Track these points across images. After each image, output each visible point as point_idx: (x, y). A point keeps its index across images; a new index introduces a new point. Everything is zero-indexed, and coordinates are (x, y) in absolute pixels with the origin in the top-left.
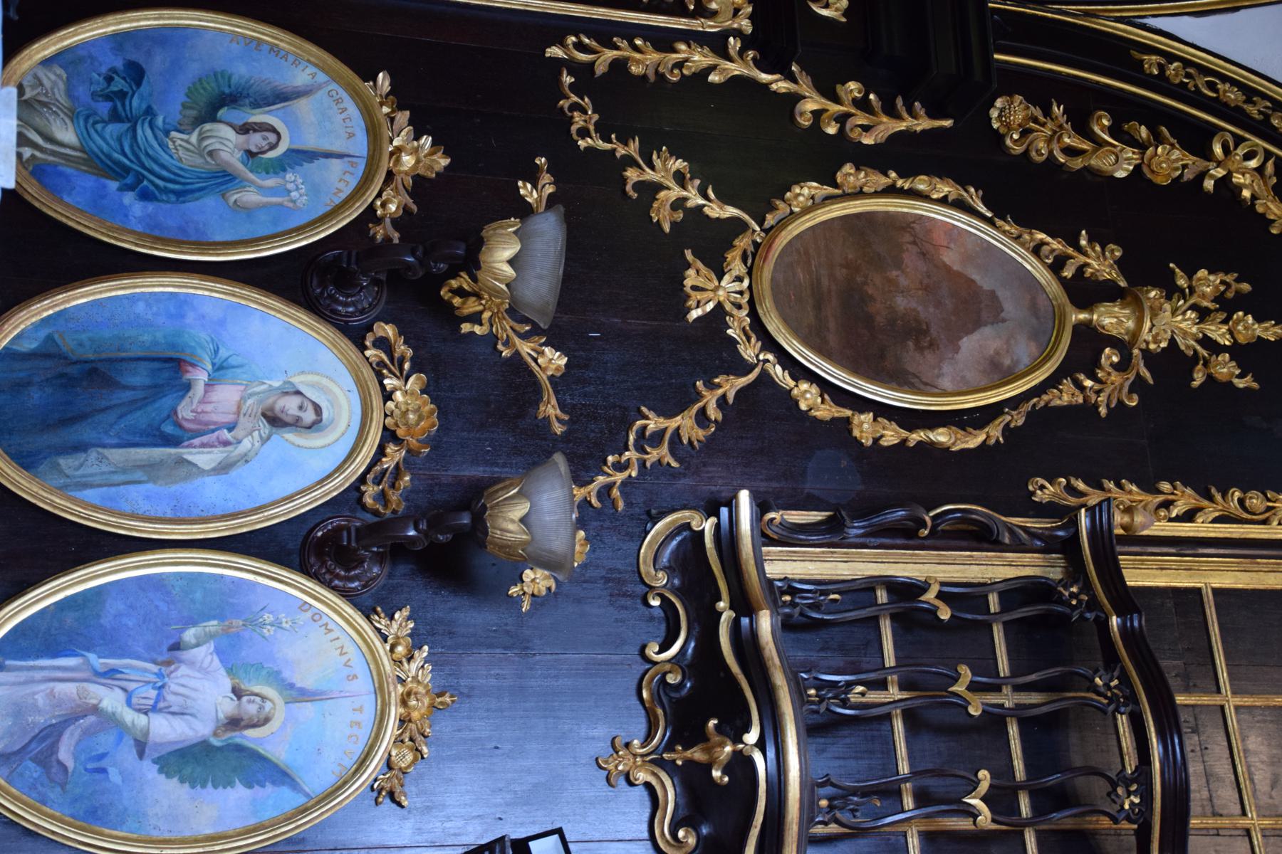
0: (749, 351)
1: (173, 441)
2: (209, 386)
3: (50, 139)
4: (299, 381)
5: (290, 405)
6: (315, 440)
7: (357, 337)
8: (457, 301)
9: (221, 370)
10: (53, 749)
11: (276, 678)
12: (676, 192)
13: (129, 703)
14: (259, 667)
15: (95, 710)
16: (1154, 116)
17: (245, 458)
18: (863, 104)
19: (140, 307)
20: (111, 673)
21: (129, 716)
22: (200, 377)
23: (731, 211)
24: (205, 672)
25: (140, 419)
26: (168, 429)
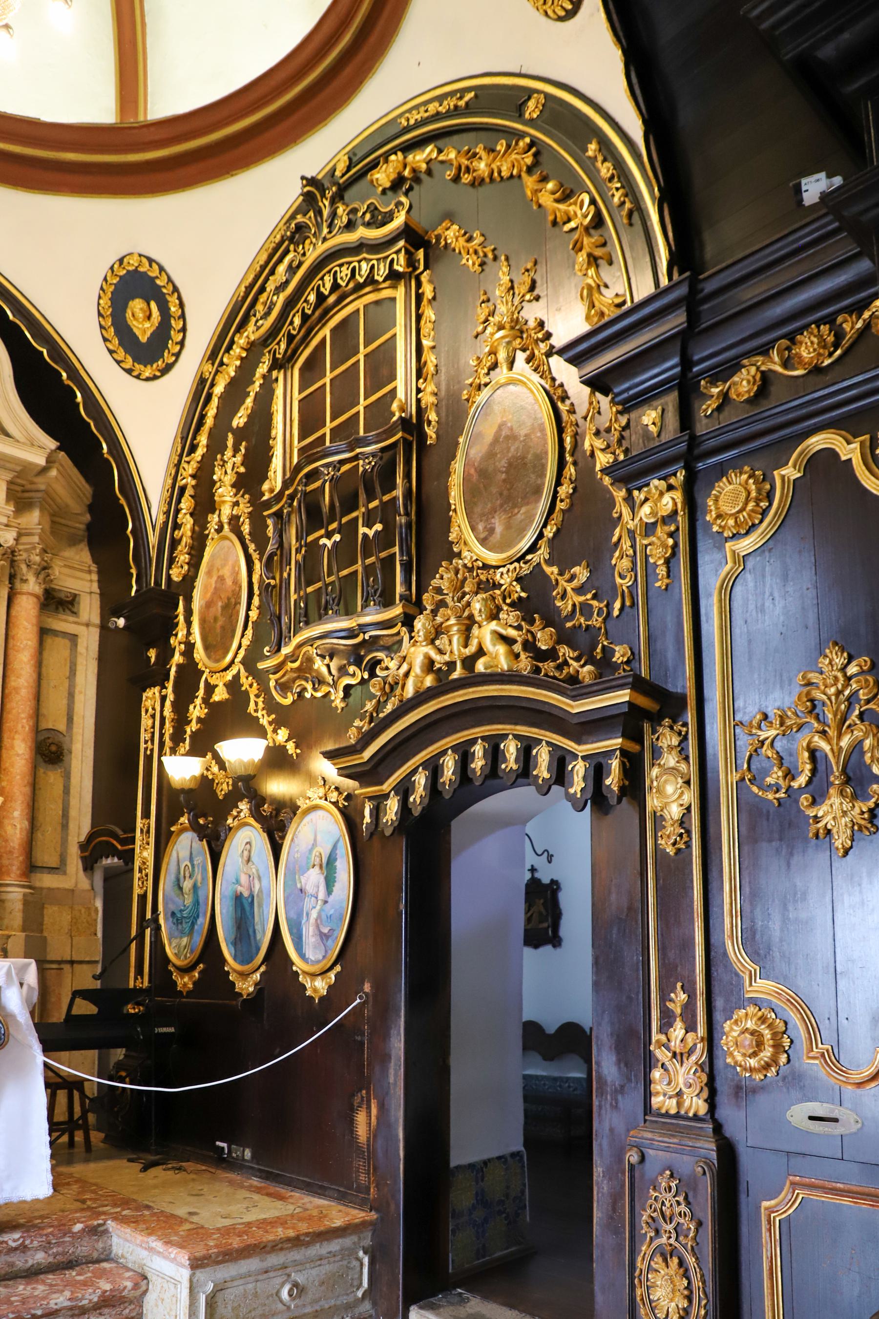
0: (233, 671)
1: (253, 897)
2: (241, 886)
3: (185, 947)
4: (240, 852)
5: (246, 853)
6: (253, 844)
7: (230, 829)
8: (223, 793)
9: (238, 882)
10: (325, 935)
11: (311, 851)
12: (198, 707)
13: (314, 907)
14: (308, 858)
15: (316, 920)
16: (177, 511)
17: (257, 870)
18: (176, 635)
19: (224, 911)
20: (307, 914)
21: (318, 907)
22: (240, 889)
23: (202, 685)
24: (308, 878)
25: (247, 908)
26: (250, 900)
